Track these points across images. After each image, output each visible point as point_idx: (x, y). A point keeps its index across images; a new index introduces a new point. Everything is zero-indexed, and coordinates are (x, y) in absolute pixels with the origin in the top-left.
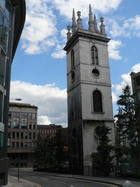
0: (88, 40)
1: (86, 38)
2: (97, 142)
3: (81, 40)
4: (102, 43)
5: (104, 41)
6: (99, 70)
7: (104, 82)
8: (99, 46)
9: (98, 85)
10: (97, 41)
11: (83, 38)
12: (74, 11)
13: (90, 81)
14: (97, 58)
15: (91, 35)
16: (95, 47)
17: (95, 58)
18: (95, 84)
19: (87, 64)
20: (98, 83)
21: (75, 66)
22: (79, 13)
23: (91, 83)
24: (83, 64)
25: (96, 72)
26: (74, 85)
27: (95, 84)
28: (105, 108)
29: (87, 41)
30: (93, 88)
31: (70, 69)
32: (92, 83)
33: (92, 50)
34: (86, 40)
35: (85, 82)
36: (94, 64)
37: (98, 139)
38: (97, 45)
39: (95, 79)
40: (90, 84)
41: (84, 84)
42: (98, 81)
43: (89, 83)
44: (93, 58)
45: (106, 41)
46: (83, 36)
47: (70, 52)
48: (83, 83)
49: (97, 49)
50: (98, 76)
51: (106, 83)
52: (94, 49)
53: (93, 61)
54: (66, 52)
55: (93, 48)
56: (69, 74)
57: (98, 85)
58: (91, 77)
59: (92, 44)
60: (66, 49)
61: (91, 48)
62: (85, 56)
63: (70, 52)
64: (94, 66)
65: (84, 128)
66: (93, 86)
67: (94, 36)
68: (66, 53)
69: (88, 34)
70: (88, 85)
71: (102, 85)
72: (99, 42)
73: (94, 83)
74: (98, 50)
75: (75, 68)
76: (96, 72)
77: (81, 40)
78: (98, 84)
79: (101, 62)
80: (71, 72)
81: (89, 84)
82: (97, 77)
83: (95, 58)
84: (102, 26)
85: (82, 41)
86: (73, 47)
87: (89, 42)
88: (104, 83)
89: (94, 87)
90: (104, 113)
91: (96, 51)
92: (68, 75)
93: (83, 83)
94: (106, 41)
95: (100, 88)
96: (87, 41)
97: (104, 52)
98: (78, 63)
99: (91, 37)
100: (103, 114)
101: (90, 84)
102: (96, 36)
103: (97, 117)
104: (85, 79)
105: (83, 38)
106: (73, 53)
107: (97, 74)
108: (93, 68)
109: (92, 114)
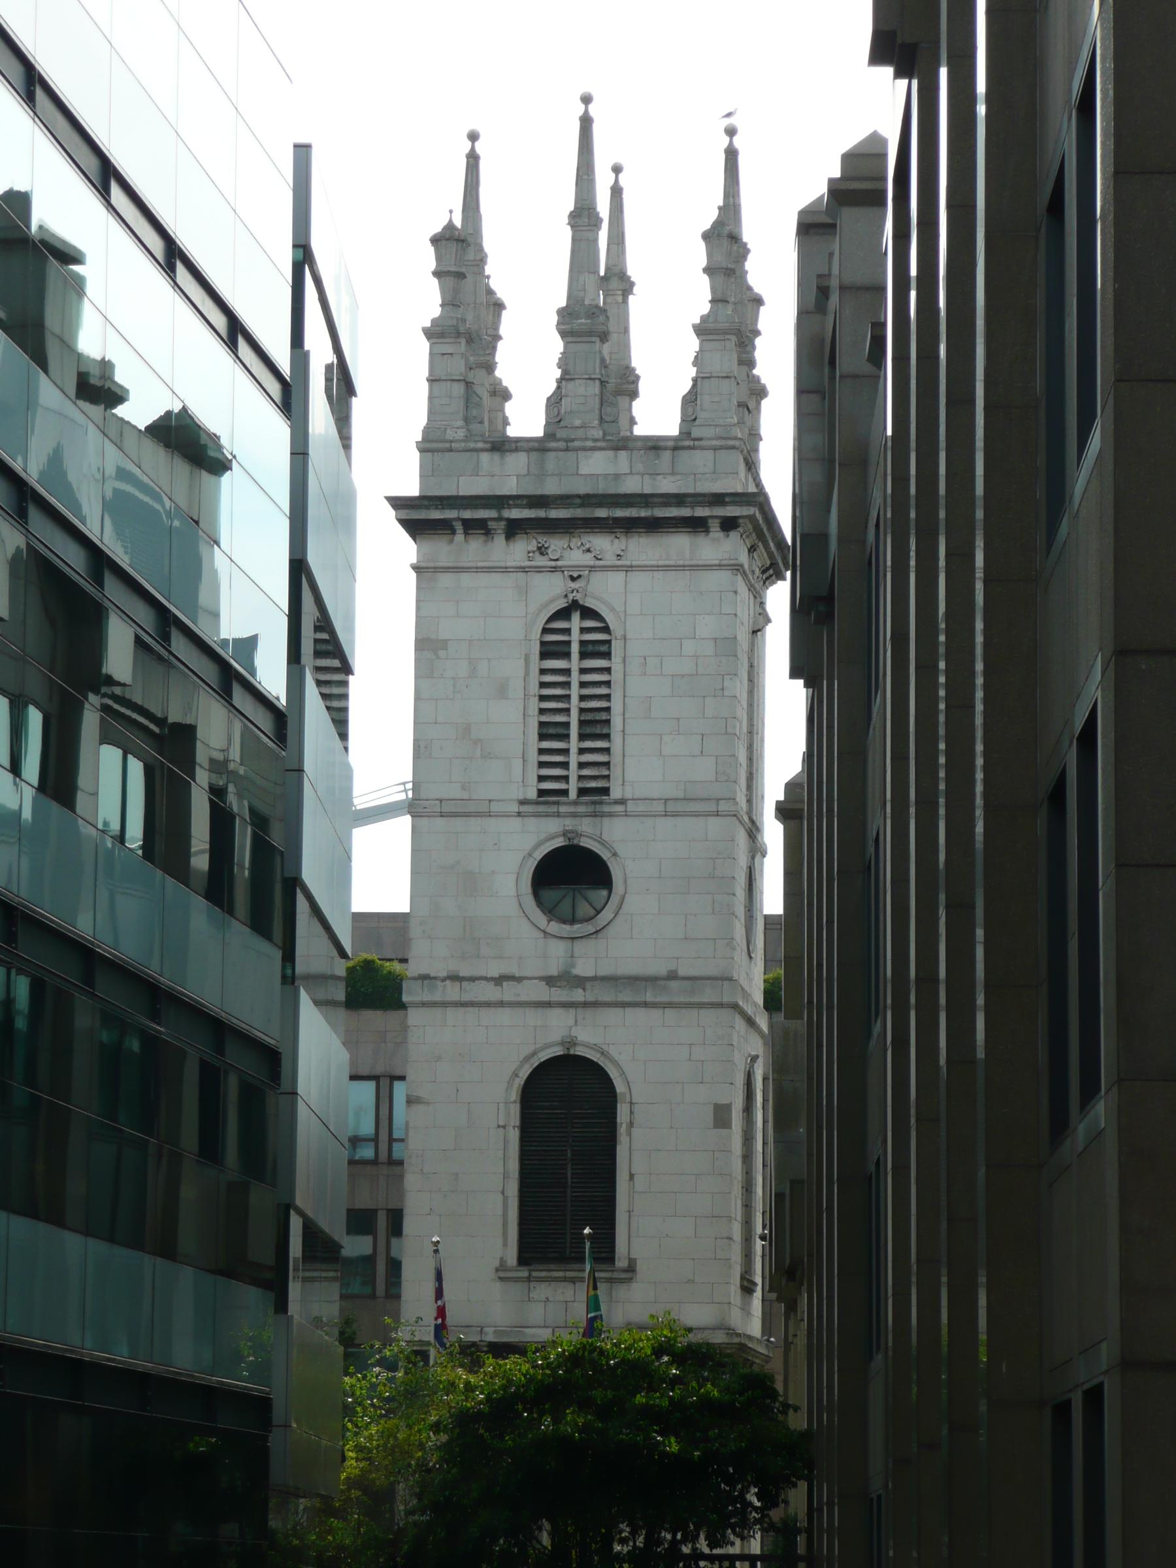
6: (605, 855)
9: (585, 1005)
13: (499, 980)
32: (523, 998)
35: (452, 992)
39: (558, 949)
40: (501, 1004)
41: (438, 1011)
42: (583, 969)
57: (585, 1005)
64: (558, 815)
66: (532, 1017)
78: (578, 995)
101: (501, 1004)
104: (454, 966)
109: (498, 1285)
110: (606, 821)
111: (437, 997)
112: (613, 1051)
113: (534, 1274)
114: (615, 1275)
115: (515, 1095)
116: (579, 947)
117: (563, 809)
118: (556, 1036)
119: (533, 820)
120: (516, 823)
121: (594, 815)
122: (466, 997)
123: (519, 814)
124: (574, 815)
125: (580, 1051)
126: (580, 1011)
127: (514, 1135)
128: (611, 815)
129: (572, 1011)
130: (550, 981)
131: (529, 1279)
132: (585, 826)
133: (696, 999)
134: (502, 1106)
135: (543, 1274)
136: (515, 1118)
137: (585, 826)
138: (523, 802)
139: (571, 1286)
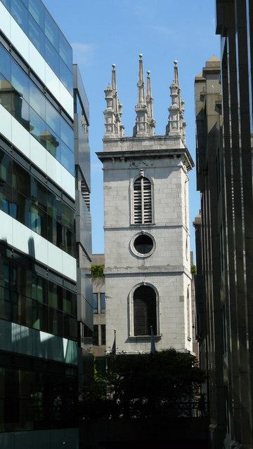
0: (128, 164)
1: (121, 160)
14: (149, 206)
17: (144, 207)
25: (144, 243)
28: (164, 326)
30: (131, 284)
35: (115, 271)
36: (141, 222)
42: (147, 265)
45: (175, 156)
49: (149, 183)
51: (168, 265)
52: (143, 185)
55: (140, 183)
58: (132, 260)
62: (117, 208)
72: (157, 163)
73: (138, 271)
76: (144, 243)
78: (146, 271)
83: (144, 207)
87: (129, 169)
91: (148, 188)
97: (170, 187)
130: (139, 268)
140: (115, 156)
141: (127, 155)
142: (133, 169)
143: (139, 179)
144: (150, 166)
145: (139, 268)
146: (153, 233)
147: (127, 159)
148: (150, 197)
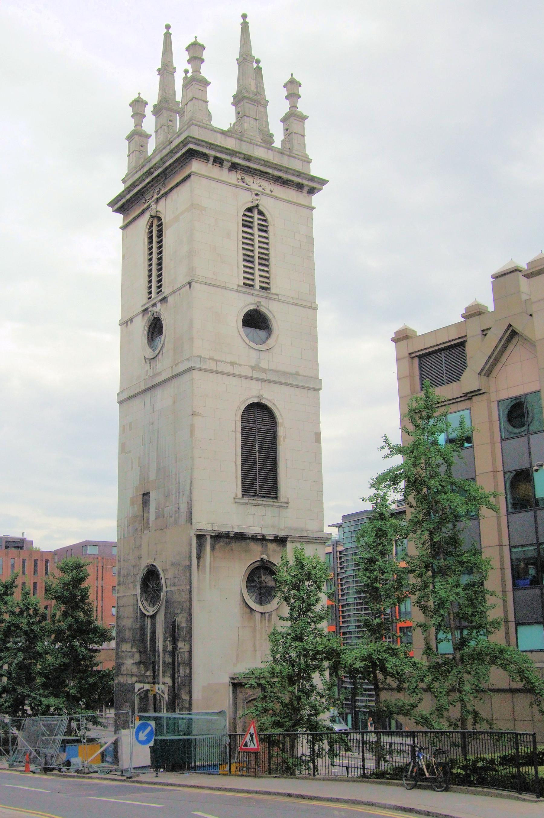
0: (233, 177)
2: (254, 629)
3: (201, 176)
4: (290, 194)
5: (300, 187)
7: (293, 371)
8: (277, 204)
9: (266, 381)
10: (267, 186)
11: (210, 165)
12: (168, 37)
13: (232, 364)
14: (265, 261)
15: (248, 158)
16: (260, 213)
17: (256, 262)
18: (251, 378)
19: (225, 288)
20: (264, 371)
21: (166, 290)
22: (196, 51)
23: (236, 370)
24: (206, 284)
26: (159, 374)
27: (251, 378)
29: (229, 184)
31: (140, 299)
32: (242, 373)
33: (248, 225)
34: (224, 174)
35: (213, 366)
37: (258, 616)
38: (266, 204)
39: (254, 354)
40: (232, 375)
42: (264, 365)
43: (229, 369)
44: (248, 259)
45: (306, 189)
46: (212, 159)
47: (143, 223)
48: (201, 370)
49: (265, 221)
50: (264, 342)
51: (297, 374)
52: (256, 222)
53: (249, 272)
54: (120, 216)
56: (131, 320)
57: (266, 381)
59: (247, 199)
60: (125, 205)
61: (244, 215)
63: (143, 223)
64: (252, 295)
65: (198, 566)
66: (245, 383)
67: (258, 160)
68: (121, 224)
69: (233, 153)
70: (225, 377)
71: (280, 383)
72: (279, 190)
73: (250, 373)
74: (270, 229)
75: (164, 300)
77: (201, 176)
78: (263, 376)
79: (281, 279)
80: (145, 311)
81: (227, 374)
82: (260, 347)
83: (256, 262)
84: (294, 118)
85: (204, 181)
86: (157, 201)
87: (236, 186)
88: (290, 374)
89: (253, 393)
90: (285, 506)
91: (264, 229)
92: (126, 323)
93: (201, 370)
94: (306, 189)
95: (272, 397)
96: (229, 184)
98: (182, 280)
99: (244, 167)
100: (280, 507)
101: (232, 375)
102: (266, 163)
103: (256, 519)
105: (210, 165)
106: (157, 231)
107: (262, 334)
108: (245, 303)
110: (270, 301)
111: (206, 367)
112: (276, 403)
113: (250, 501)
114: (282, 504)
115: (239, 418)
116: (262, 354)
117: (255, 292)
118: (254, 393)
119: (242, 295)
120: (235, 294)
121: (266, 298)
122: (219, 369)
123: (237, 291)
124: (259, 296)
125: (264, 402)
126: (263, 383)
127: (239, 436)
128: (273, 299)
129: (260, 383)
130: (253, 368)
131: (247, 504)
132: (263, 302)
133: (308, 385)
134: (234, 422)
135: (254, 502)
136: (239, 429)
137: (263, 302)
138: (239, 286)
139: (263, 508)
140: (219, 155)
141: (237, 160)
142: (242, 188)
143: (250, 210)
144: (267, 191)
145: (253, 368)
146: (272, 309)
147: (234, 167)
148: (265, 244)
